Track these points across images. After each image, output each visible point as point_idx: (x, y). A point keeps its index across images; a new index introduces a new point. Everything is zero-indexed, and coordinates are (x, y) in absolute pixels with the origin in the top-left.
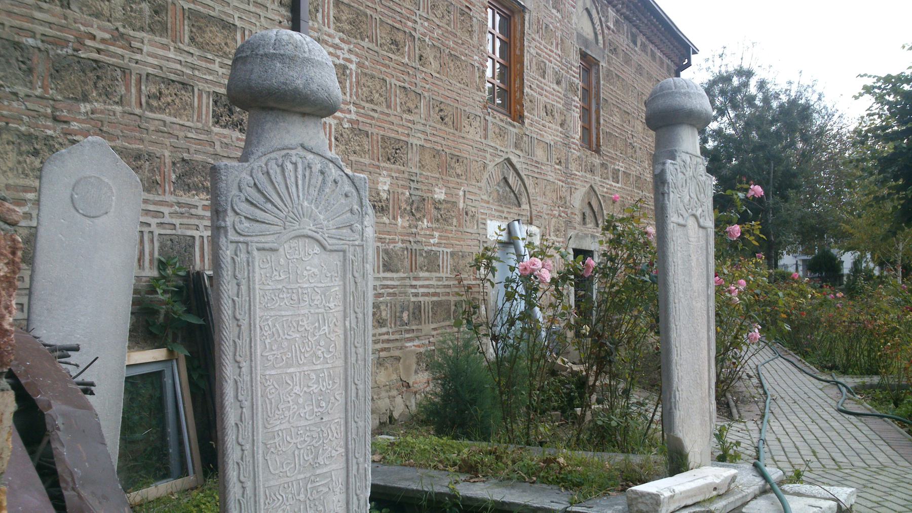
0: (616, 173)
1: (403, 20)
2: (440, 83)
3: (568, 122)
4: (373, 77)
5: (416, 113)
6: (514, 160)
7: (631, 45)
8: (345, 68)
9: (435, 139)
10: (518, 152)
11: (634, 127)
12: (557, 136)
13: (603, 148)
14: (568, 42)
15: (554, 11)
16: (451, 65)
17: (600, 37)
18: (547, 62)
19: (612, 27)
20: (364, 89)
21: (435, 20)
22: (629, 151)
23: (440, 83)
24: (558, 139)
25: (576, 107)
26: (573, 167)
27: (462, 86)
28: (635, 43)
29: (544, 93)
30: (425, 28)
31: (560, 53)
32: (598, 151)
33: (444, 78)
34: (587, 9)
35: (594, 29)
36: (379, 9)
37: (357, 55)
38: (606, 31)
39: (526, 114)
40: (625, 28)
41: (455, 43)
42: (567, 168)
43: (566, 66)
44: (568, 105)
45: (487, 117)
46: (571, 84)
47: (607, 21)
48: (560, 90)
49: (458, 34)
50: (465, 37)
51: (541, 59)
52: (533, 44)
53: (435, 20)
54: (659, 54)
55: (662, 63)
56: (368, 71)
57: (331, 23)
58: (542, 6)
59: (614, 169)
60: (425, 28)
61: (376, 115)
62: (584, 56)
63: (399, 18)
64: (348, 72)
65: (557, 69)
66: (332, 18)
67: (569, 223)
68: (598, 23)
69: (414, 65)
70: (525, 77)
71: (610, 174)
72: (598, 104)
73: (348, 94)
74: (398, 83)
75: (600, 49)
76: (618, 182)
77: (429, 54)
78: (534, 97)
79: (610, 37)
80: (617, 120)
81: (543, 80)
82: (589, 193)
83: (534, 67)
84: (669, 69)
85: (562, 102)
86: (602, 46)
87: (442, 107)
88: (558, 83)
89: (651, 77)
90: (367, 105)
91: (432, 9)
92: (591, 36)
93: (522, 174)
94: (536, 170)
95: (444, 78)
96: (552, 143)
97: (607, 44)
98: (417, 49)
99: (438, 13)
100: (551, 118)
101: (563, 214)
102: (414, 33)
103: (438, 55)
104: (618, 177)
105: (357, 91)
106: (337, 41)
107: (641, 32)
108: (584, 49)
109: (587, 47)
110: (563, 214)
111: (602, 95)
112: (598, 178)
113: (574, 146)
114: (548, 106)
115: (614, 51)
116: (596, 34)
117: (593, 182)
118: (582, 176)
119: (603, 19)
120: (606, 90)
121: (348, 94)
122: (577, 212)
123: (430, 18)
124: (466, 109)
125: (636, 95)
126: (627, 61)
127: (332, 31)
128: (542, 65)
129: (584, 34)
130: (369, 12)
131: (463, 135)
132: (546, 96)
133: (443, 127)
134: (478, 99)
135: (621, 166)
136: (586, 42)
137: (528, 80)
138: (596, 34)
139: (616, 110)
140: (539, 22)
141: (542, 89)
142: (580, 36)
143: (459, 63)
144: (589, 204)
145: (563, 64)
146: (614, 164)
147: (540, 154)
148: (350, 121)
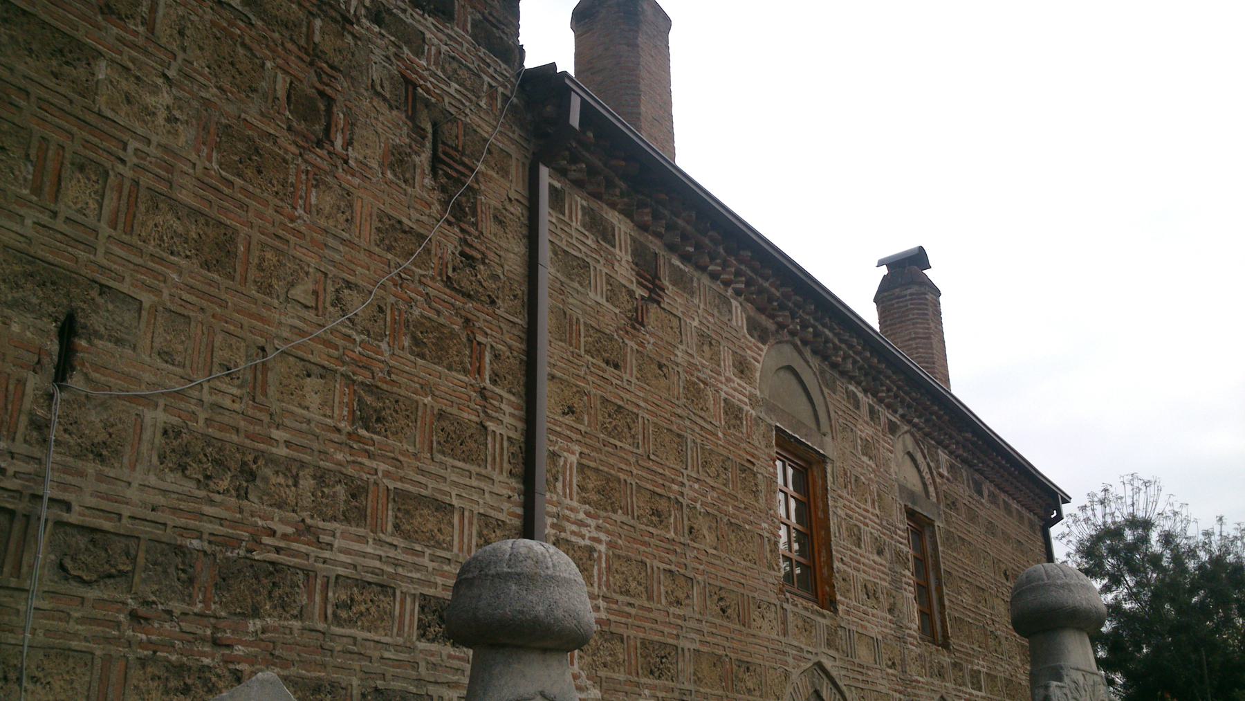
0: (975, 675)
1: (667, 483)
2: (718, 562)
3: (899, 606)
4: (628, 559)
5: (687, 605)
6: (828, 664)
8: (591, 550)
9: (715, 641)
11: (993, 608)
12: (886, 627)
13: (952, 640)
15: (865, 459)
16: (732, 536)
17: (931, 489)
18: (862, 526)
19: (946, 474)
21: (708, 480)
22: (991, 642)
23: (718, 562)
24: (887, 631)
25: (909, 584)
26: (913, 671)
27: (749, 564)
28: (980, 493)
30: (695, 491)
31: (877, 512)
32: (946, 645)
33: (723, 555)
34: (909, 453)
35: (922, 478)
36: (635, 472)
37: (607, 532)
38: (938, 480)
39: (838, 597)
40: (964, 474)
41: (735, 507)
42: (904, 672)
43: (889, 530)
44: (896, 582)
45: (785, 606)
46: (898, 553)
47: (938, 467)
49: (739, 496)
50: (749, 499)
52: (840, 503)
53: (708, 480)
54: (1015, 505)
55: (1021, 517)
56: (623, 553)
57: (574, 494)
58: (847, 452)
59: (972, 670)
60: (695, 491)
61: (633, 611)
62: (911, 514)
63: (661, 481)
64: (596, 555)
65: (876, 534)
66: (575, 488)
68: (927, 470)
69: (682, 540)
70: (834, 547)
71: (968, 678)
72: (938, 579)
73: (596, 585)
74: (662, 566)
76: (980, 690)
77: (703, 525)
78: (848, 574)
79: (945, 487)
80: (967, 599)
81: (858, 550)
83: (845, 534)
84: (1032, 525)
87: (723, 594)
88: (880, 552)
90: (621, 598)
91: (703, 467)
92: (917, 487)
93: (841, 684)
94: (860, 677)
95: (723, 555)
96: (880, 638)
97: (942, 497)
98: (686, 519)
99: (712, 471)
100: (874, 602)
102: (681, 499)
103: (714, 525)
104: (979, 682)
105: (608, 580)
106: (582, 516)
108: (910, 505)
109: (914, 503)
111: (942, 566)
114: (869, 586)
115: (953, 505)
116: (924, 484)
117: (944, 691)
119: (932, 464)
120: (948, 559)
121: (596, 585)
123: (702, 478)
124: (756, 595)
125: (990, 563)
126: (973, 518)
127: (575, 504)
128: (855, 530)
129: (909, 486)
130: (622, 476)
131: (754, 632)
133: (725, 623)
134: (770, 580)
135: (981, 665)
136: (912, 495)
137: (837, 551)
138: (924, 484)
139: (964, 585)
140: (846, 474)
141: (858, 562)
142: (902, 488)
143: (742, 534)
145: (884, 527)
146: (972, 663)
147: (863, 654)
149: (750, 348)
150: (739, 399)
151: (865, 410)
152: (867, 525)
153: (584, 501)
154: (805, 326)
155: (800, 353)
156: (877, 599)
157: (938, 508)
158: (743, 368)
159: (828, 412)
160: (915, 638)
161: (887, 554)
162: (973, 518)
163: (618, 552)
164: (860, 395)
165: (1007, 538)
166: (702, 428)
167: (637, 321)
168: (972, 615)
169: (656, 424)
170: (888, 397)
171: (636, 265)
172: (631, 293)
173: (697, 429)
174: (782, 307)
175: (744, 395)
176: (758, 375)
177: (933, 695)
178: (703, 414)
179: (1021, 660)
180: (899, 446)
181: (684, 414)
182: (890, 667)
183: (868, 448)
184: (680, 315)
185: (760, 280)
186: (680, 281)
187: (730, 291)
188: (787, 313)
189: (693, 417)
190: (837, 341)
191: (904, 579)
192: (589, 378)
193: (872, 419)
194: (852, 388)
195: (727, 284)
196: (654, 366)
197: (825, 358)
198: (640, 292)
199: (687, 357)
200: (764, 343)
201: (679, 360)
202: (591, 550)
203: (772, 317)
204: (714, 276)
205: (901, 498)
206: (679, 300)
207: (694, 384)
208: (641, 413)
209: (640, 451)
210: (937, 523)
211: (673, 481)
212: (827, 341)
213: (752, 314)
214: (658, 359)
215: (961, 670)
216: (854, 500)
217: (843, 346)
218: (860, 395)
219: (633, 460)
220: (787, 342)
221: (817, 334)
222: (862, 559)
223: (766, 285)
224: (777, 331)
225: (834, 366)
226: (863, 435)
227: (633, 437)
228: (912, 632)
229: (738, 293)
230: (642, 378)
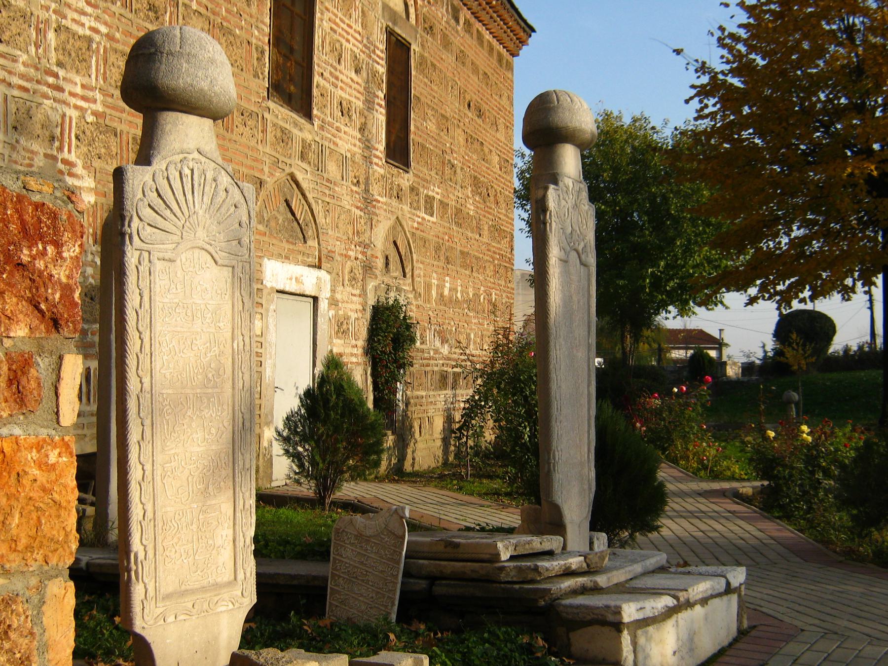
0: (429, 200)
3: (369, 126)
6: (300, 177)
8: (90, 40)
10: (305, 165)
11: (453, 138)
12: (355, 145)
14: (371, 15)
20: (114, 70)
22: (448, 171)
24: (356, 149)
26: (375, 190)
29: (340, 84)
31: (360, 29)
42: (367, 191)
43: (368, 48)
44: (369, 104)
46: (375, 74)
51: (336, 37)
59: (427, 196)
64: (94, 46)
65: (357, 51)
67: (368, 268)
71: (422, 202)
73: (93, 76)
75: (411, 26)
80: (431, 126)
81: (338, 66)
88: (357, 71)
93: (310, 196)
94: (327, 192)
96: (349, 155)
101: (360, 256)
105: (105, 73)
108: (390, 24)
109: (395, 23)
110: (360, 256)
112: (406, 208)
113: (375, 160)
115: (430, 30)
118: (385, 204)
120: (418, 84)
121: (93, 76)
122: (379, 255)
131: (234, 137)
135: (436, 192)
136: (392, 15)
139: (430, 112)
146: (428, 188)
147: (332, 169)
152: (348, 41)
157: (417, 32)
160: (381, 159)
162: (446, 44)
163: (115, 45)
168: (434, 143)
177: (389, 216)
179: (472, 191)
182: (355, 185)
202: (90, 40)
205: (383, 17)
210: (413, 47)
215: (417, 195)
228: (378, 153)
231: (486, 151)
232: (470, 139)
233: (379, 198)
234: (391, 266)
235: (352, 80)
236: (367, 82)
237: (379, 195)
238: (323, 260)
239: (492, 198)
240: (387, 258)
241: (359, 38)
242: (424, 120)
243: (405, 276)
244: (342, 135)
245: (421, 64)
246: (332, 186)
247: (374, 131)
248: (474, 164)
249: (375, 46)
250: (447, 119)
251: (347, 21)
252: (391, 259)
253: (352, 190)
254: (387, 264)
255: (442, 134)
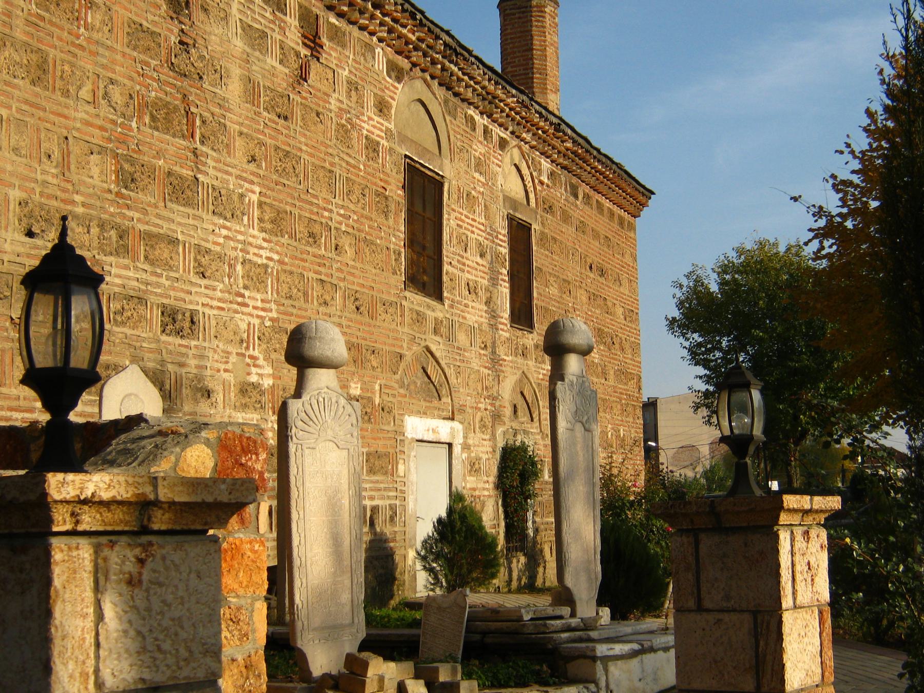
1: (320, 211)
3: (494, 299)
4: (291, 273)
5: (332, 305)
6: (433, 348)
7: (572, 199)
10: (438, 338)
11: (576, 298)
12: (482, 317)
14: (493, 207)
15: (477, 175)
16: (367, 250)
17: (532, 196)
18: (469, 233)
19: (546, 181)
25: (504, 281)
26: (501, 351)
28: (576, 197)
30: (341, 215)
31: (483, 221)
34: (515, 165)
35: (525, 186)
36: (298, 204)
37: (277, 253)
40: (563, 179)
42: (494, 352)
43: (491, 235)
45: (404, 303)
47: (540, 174)
48: (485, 263)
52: (454, 215)
54: (607, 204)
56: (288, 268)
57: (256, 224)
60: (341, 215)
61: (295, 311)
63: (315, 210)
64: (270, 270)
66: (256, 221)
67: (497, 417)
69: (330, 255)
70: (444, 252)
74: (315, 276)
75: (531, 210)
77: (345, 242)
80: (554, 291)
82: (521, 380)
83: (455, 241)
85: (487, 277)
86: (534, 205)
87: (358, 295)
89: (598, 234)
90: (287, 302)
91: (348, 195)
92: (519, 194)
93: (443, 363)
94: (458, 358)
96: (476, 325)
97: (540, 201)
98: (333, 238)
100: (474, 296)
101: (489, 407)
102: (330, 223)
106: (260, 242)
107: (583, 181)
108: (511, 212)
109: (515, 210)
110: (489, 407)
112: (531, 363)
113: (501, 326)
114: (471, 284)
117: (525, 368)
118: (511, 362)
119: (535, 174)
122: (507, 405)
125: (578, 258)
126: (566, 218)
127: (256, 232)
128: (464, 238)
130: (288, 208)
132: (468, 272)
133: (359, 317)
139: (552, 279)
140: (459, 190)
141: (464, 264)
142: (507, 199)
143: (374, 247)
144: (522, 393)
147: (462, 338)
148: (271, 319)
149: (388, 89)
150: (377, 135)
151: (480, 131)
152: (473, 232)
153: (262, 230)
154: (434, 62)
155: (428, 86)
156: (476, 294)
158: (382, 108)
159: (449, 136)
160: (506, 325)
161: (488, 257)
163: (285, 267)
164: (477, 118)
165: (596, 235)
166: (347, 163)
167: (303, 76)
168: (557, 305)
169: (313, 164)
170: (501, 117)
171: (302, 27)
172: (298, 54)
173: (344, 165)
174: (416, 49)
175: (381, 130)
176: (393, 111)
178: (349, 151)
180: (507, 160)
181: (335, 153)
182: (483, 349)
183: (479, 166)
184: (335, 68)
185: (400, 29)
186: (336, 35)
187: (375, 39)
188: (420, 54)
189: (342, 155)
190: (460, 73)
191: (500, 277)
192: (266, 131)
193: (485, 139)
194: (471, 112)
195: (372, 34)
196: (314, 115)
197: (449, 88)
198: (304, 52)
199: (338, 104)
200: (399, 82)
201: (333, 107)
202: (266, 266)
203: (408, 57)
204: (362, 28)
205: (504, 207)
206: (334, 54)
207: (343, 126)
208: (304, 156)
209: (301, 187)
211: (325, 209)
212: (452, 74)
213: (391, 57)
214: (316, 108)
216: (465, 212)
217: (466, 78)
218: (477, 118)
219: (296, 195)
220: (418, 78)
221: (443, 69)
222: (467, 262)
223: (405, 31)
224: (411, 70)
225: (456, 95)
226: (477, 154)
227: (297, 176)
228: (503, 321)
229: (381, 40)
230: (305, 126)
231: (610, 304)
232: (593, 297)
233: (505, 358)
234: (519, 413)
235: (477, 263)
236: (492, 263)
237: (506, 355)
238: (456, 413)
239: (617, 346)
240: (515, 406)
241: (483, 228)
242: (546, 286)
243: (532, 420)
244: (470, 309)
245: (541, 240)
246: (462, 352)
247: (499, 303)
248: (597, 318)
249: (498, 232)
250: (569, 283)
251: (471, 216)
252: (519, 407)
253: (480, 354)
254: (515, 412)
255: (564, 296)
